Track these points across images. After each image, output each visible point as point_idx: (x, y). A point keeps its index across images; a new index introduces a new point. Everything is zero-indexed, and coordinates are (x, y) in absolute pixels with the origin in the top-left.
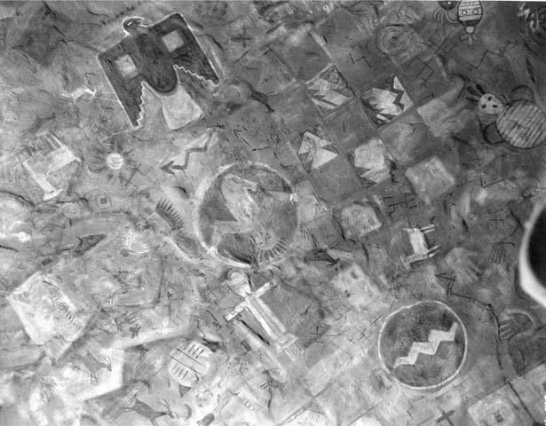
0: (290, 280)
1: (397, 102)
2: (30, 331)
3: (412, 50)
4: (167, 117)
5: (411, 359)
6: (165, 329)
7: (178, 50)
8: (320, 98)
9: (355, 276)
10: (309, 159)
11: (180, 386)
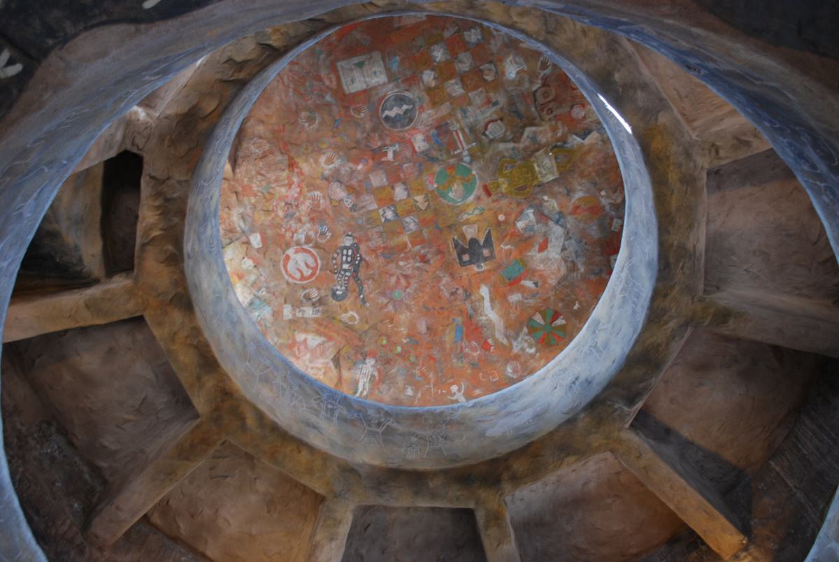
1: (385, 213)
2: (554, 161)
5: (405, 107)
6: (502, 146)
7: (465, 253)
8: (415, 222)
9: (419, 148)
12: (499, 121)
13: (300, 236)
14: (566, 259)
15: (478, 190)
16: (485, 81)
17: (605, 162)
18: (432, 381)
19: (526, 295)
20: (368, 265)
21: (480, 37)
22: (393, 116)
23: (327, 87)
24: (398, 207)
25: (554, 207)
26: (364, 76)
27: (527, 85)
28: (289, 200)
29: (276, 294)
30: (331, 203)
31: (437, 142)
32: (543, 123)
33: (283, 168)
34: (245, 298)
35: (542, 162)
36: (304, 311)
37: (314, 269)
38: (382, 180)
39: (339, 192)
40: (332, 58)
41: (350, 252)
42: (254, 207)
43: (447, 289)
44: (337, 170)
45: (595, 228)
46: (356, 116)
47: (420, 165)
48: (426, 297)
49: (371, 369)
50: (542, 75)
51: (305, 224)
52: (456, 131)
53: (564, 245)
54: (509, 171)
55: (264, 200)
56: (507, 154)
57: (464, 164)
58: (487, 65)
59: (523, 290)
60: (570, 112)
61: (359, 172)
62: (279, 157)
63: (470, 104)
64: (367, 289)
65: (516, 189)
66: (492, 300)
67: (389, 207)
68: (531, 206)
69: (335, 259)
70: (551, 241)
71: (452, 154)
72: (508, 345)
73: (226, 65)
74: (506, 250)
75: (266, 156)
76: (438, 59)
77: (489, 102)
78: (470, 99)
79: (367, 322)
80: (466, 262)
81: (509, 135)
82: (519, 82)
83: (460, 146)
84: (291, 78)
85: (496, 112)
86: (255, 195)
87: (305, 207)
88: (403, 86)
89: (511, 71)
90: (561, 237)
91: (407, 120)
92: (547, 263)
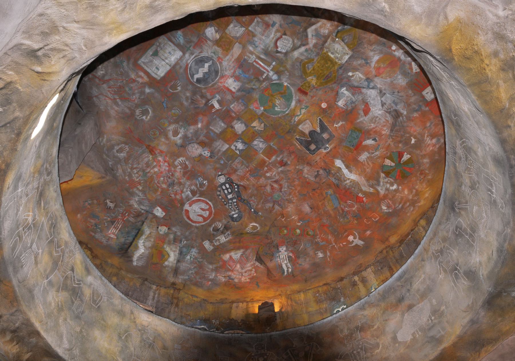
0: (256, 81)
1: (236, 147)
2: (342, 44)
3: (236, 163)
5: (207, 65)
6: (296, 54)
7: (311, 145)
8: (263, 141)
9: (234, 88)
11: (286, 35)
12: (283, 36)
13: (187, 193)
14: (389, 110)
15: (296, 97)
18: (333, 240)
19: (371, 151)
20: (245, 188)
22: (202, 76)
25: (360, 78)
26: (163, 60)
29: (194, 238)
33: (147, 155)
34: (174, 251)
35: (334, 49)
36: (219, 240)
37: (210, 209)
38: (221, 125)
39: (195, 150)
40: (132, 61)
41: (228, 186)
42: (143, 191)
43: (310, 175)
44: (185, 137)
45: (399, 77)
46: (175, 91)
48: (299, 188)
49: (286, 253)
51: (185, 183)
52: (255, 61)
53: (382, 101)
56: (303, 58)
57: (274, 82)
59: (367, 148)
64: (253, 204)
65: (324, 80)
66: (347, 167)
67: (237, 142)
68: (343, 86)
69: (220, 195)
70: (371, 103)
72: (375, 191)
74: (339, 127)
77: (268, 26)
78: (253, 33)
79: (266, 225)
80: (314, 150)
81: (298, 43)
83: (265, 71)
84: (113, 93)
85: (277, 31)
86: (140, 184)
87: (178, 172)
88: (197, 52)
90: (377, 96)
92: (376, 121)
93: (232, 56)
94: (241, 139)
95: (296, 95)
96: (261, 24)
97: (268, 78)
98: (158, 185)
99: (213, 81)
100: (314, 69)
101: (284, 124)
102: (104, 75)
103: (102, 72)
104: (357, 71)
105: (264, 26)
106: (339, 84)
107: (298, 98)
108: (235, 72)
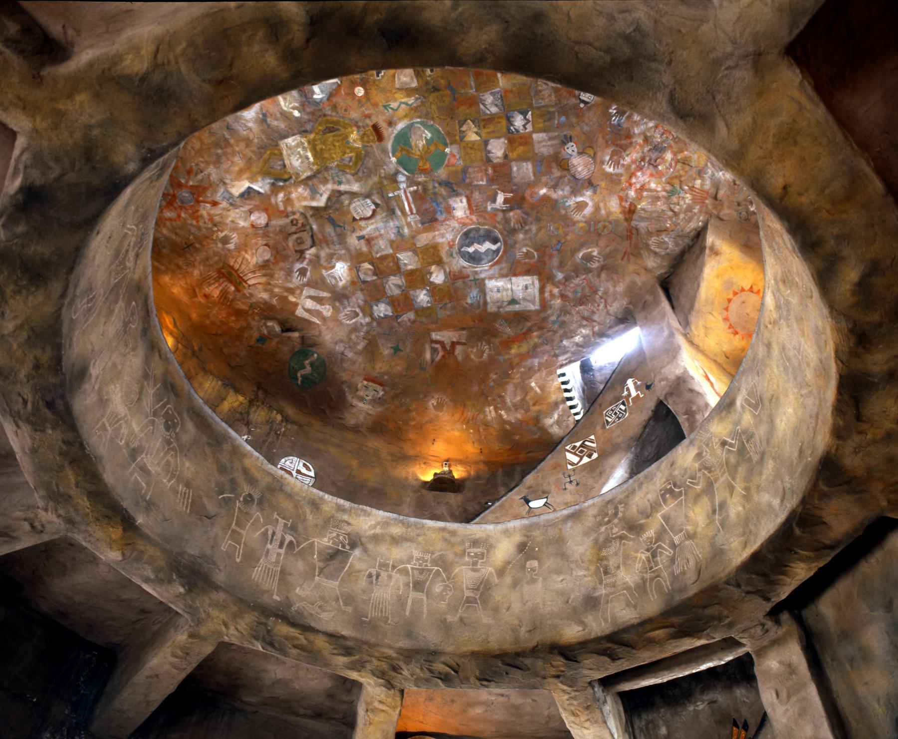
1: (524, 126)
2: (287, 162)
3: (546, 100)
4: (396, 80)
5: (471, 250)
6: (356, 187)
9: (461, 202)
10: (464, 134)
12: (358, 218)
15: (391, 134)
16: (371, 263)
17: (219, 157)
21: (375, 308)
23: (558, 287)
24: (505, 130)
26: (512, 290)
27: (323, 254)
28: (651, 170)
30: (595, 154)
31: (437, 205)
32: (301, 210)
35: (302, 162)
38: (518, 170)
39: (580, 165)
40: (543, 315)
42: (700, 173)
44: (575, 192)
46: (532, 251)
47: (464, 180)
50: (305, 263)
51: (640, 134)
54: (346, 155)
55: (683, 179)
56: (349, 176)
58: (369, 279)
60: (270, 219)
61: (546, 185)
62: (642, 225)
63: (392, 242)
65: (338, 130)
67: (517, 131)
68: (316, 103)
71: (420, 187)
73: (620, 656)
75: (658, 231)
76: (424, 292)
77: (369, 241)
78: (391, 246)
81: (346, 200)
82: (331, 257)
83: (409, 195)
85: (361, 229)
86: (692, 188)
88: (469, 271)
89: (341, 270)
91: (471, 235)
93: (434, 237)
94: (509, 129)
95: (389, 136)
96: (375, 248)
97: (411, 182)
98: (673, 164)
99: (479, 228)
100: (344, 153)
101: (433, 107)
102: (584, 327)
103: (584, 331)
104: (285, 112)
105: (373, 243)
106: (320, 110)
107: (390, 129)
108: (446, 219)
